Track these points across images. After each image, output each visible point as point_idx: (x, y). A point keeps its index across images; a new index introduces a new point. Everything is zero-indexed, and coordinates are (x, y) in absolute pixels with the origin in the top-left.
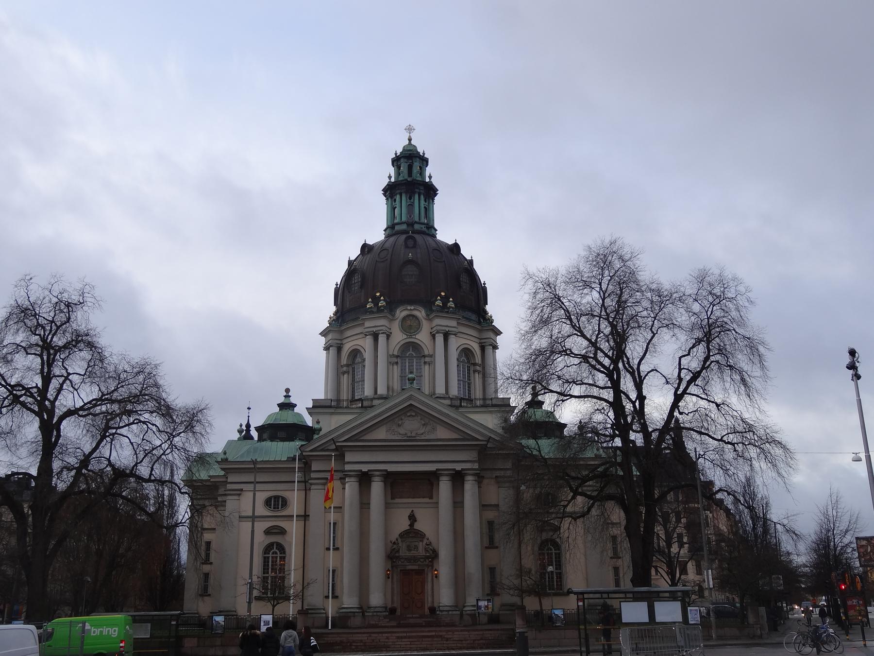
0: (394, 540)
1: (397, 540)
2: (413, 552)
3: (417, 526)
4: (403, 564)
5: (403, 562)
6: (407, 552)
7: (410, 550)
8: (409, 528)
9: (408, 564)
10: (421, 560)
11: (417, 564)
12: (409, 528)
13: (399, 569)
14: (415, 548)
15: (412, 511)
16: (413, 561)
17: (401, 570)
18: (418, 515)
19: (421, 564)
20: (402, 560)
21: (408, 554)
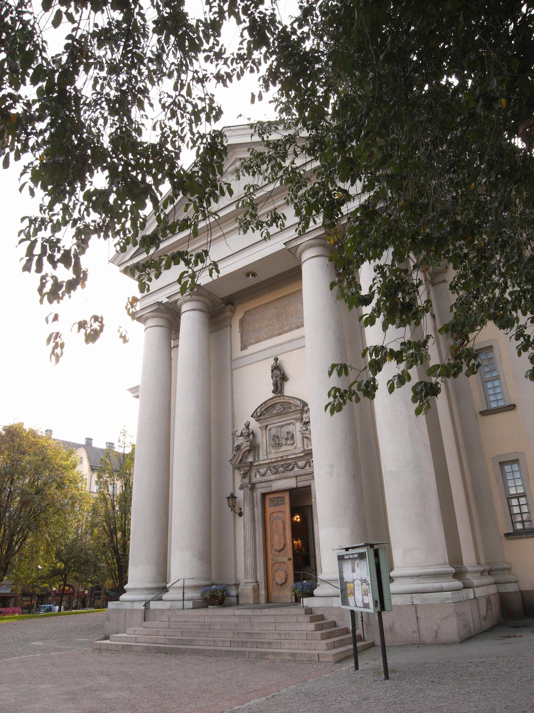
0: (240, 428)
1: (247, 426)
2: (284, 448)
3: (290, 390)
4: (264, 479)
5: (264, 475)
6: (273, 451)
7: (280, 445)
8: (272, 395)
9: (273, 477)
10: (301, 463)
11: (291, 473)
12: (272, 395)
13: (258, 494)
14: (287, 439)
15: (276, 359)
16: (281, 469)
17: (264, 495)
18: (289, 369)
19: (302, 472)
20: (262, 471)
21: (274, 455)
